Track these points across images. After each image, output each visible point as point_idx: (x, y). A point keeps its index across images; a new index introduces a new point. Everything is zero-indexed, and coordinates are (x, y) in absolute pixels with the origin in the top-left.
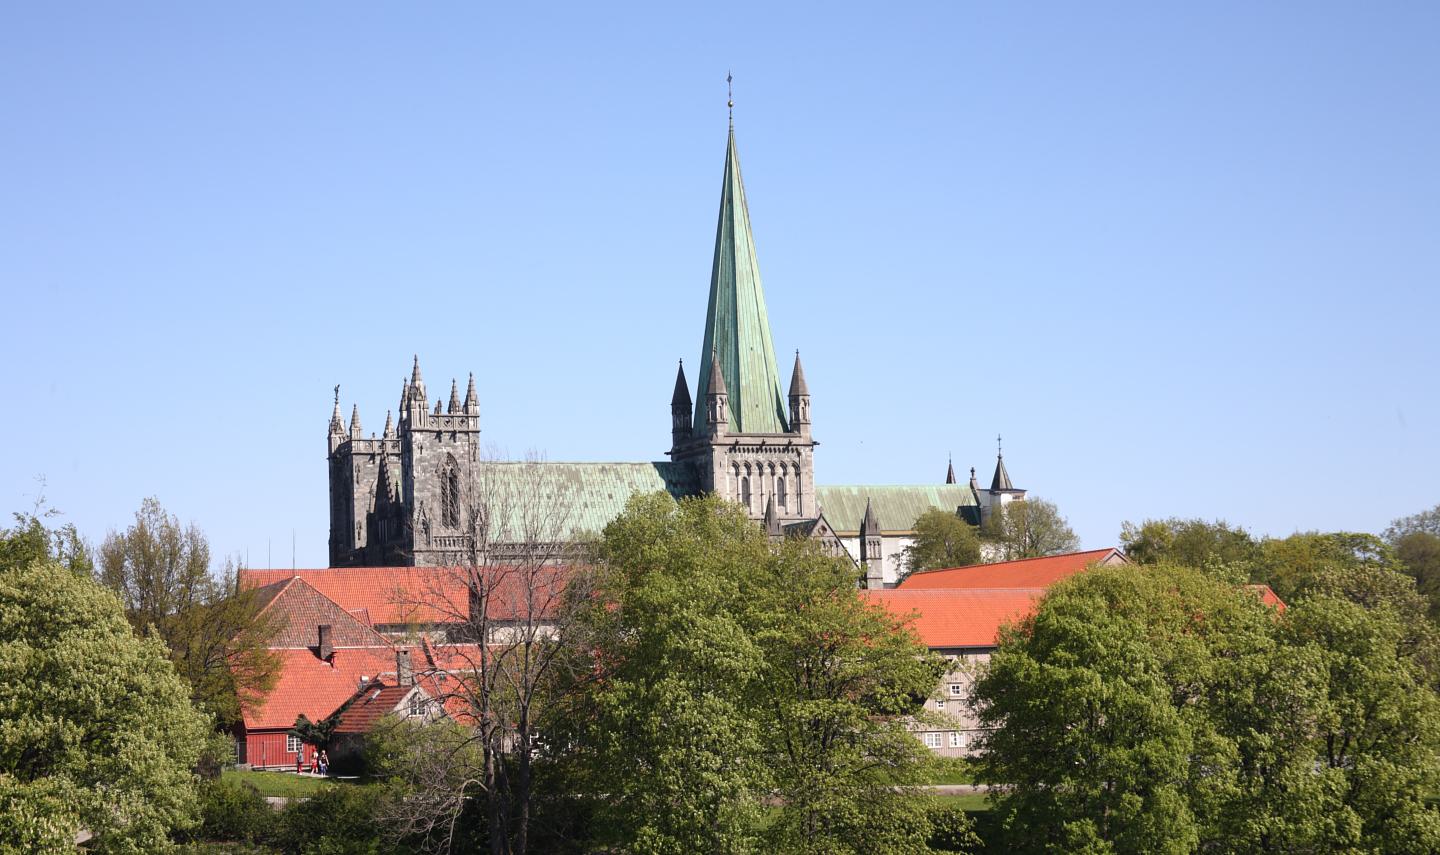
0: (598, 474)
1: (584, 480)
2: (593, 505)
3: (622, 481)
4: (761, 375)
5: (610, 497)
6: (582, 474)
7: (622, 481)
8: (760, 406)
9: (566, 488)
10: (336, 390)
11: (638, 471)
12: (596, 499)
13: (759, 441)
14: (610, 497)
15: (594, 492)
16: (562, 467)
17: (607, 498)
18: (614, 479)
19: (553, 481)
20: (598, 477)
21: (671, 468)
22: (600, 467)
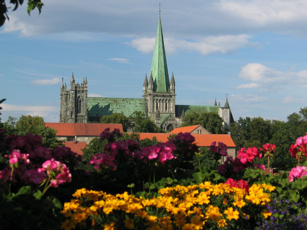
1: (118, 102)
2: (120, 108)
3: (128, 103)
4: (163, 78)
5: (124, 106)
7: (128, 103)
10: (63, 79)
11: (132, 101)
12: (121, 107)
14: (124, 106)
20: (121, 102)
21: (140, 100)
22: (123, 99)
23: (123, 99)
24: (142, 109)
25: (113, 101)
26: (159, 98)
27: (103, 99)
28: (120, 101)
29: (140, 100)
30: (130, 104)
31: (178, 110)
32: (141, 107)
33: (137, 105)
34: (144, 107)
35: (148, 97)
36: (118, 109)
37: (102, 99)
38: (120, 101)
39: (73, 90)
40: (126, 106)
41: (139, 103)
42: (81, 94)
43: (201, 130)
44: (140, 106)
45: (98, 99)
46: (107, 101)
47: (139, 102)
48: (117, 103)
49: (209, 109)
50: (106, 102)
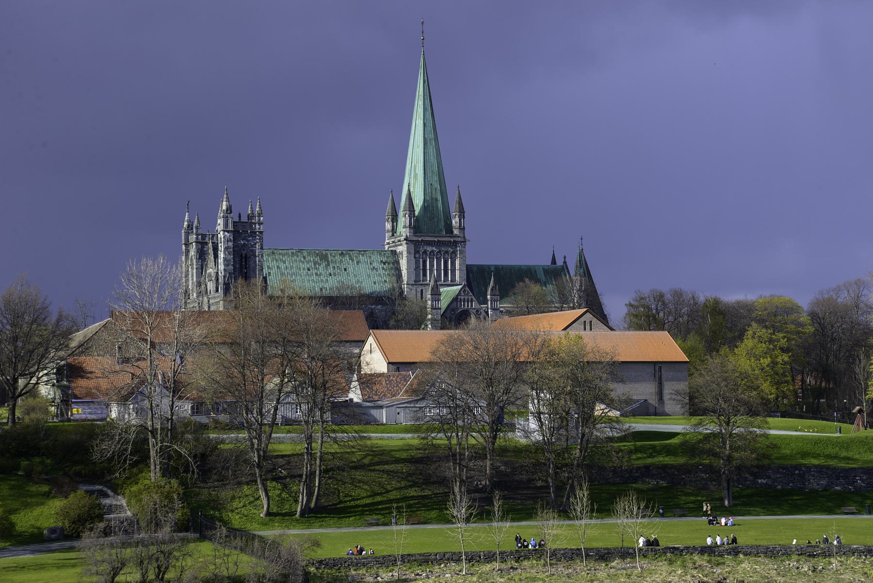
1: (330, 260)
3: (353, 261)
5: (345, 270)
6: (329, 256)
7: (353, 261)
8: (435, 218)
9: (320, 265)
11: (363, 255)
12: (337, 271)
14: (345, 270)
15: (336, 266)
16: (317, 252)
17: (343, 270)
18: (348, 259)
19: (312, 260)
20: (338, 258)
21: (383, 254)
23: (342, 253)
24: (389, 275)
27: (294, 251)
28: (334, 257)
29: (380, 254)
30: (358, 263)
31: (471, 275)
32: (386, 270)
33: (375, 265)
34: (393, 271)
35: (401, 245)
36: (330, 275)
37: (292, 253)
38: (334, 257)
39: (228, 232)
40: (350, 269)
41: (379, 261)
42: (248, 241)
43: (591, 322)
44: (383, 268)
45: (283, 252)
46: (304, 258)
47: (379, 258)
48: (328, 262)
49: (542, 273)
50: (303, 259)
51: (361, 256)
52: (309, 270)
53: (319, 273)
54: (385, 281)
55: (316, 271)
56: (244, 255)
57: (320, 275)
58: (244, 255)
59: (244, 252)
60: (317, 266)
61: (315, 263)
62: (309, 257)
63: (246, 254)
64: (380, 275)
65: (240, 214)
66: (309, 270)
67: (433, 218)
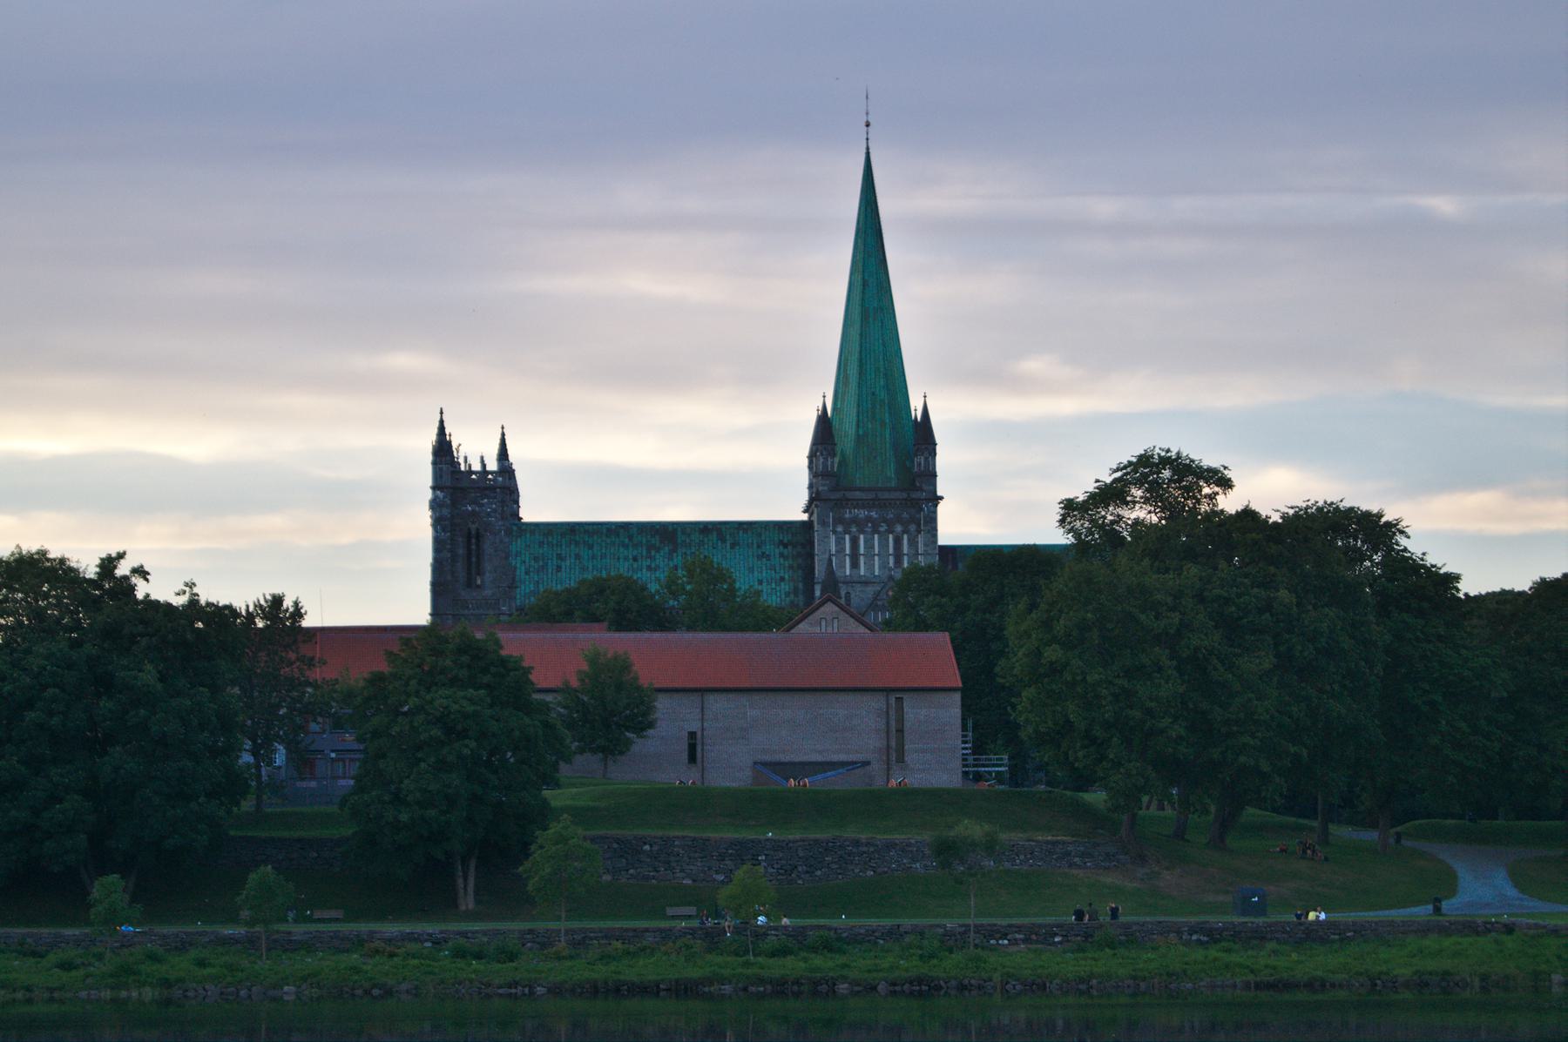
0: (697, 534)
1: (679, 541)
4: (883, 424)
6: (679, 533)
9: (658, 550)
13: (871, 496)
16: (658, 527)
18: (715, 539)
20: (696, 537)
24: (791, 567)
25: (657, 537)
26: (862, 513)
30: (733, 546)
33: (768, 548)
34: (800, 561)
44: (781, 555)
46: (630, 538)
50: (627, 541)
51: (741, 532)
52: (635, 559)
53: (653, 566)
54: (782, 579)
55: (648, 563)
56: (473, 532)
57: (657, 568)
58: (473, 532)
59: (473, 527)
60: (653, 553)
61: (650, 547)
62: (639, 536)
63: (478, 529)
64: (773, 568)
65: (482, 458)
66: (635, 559)
67: (875, 458)
